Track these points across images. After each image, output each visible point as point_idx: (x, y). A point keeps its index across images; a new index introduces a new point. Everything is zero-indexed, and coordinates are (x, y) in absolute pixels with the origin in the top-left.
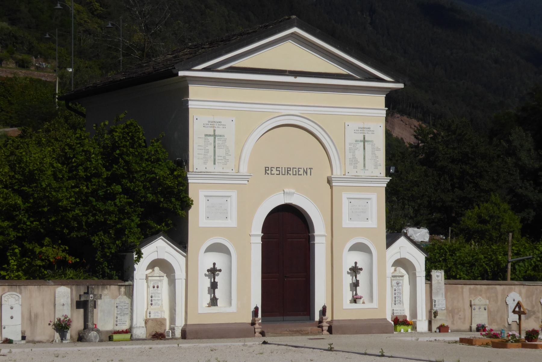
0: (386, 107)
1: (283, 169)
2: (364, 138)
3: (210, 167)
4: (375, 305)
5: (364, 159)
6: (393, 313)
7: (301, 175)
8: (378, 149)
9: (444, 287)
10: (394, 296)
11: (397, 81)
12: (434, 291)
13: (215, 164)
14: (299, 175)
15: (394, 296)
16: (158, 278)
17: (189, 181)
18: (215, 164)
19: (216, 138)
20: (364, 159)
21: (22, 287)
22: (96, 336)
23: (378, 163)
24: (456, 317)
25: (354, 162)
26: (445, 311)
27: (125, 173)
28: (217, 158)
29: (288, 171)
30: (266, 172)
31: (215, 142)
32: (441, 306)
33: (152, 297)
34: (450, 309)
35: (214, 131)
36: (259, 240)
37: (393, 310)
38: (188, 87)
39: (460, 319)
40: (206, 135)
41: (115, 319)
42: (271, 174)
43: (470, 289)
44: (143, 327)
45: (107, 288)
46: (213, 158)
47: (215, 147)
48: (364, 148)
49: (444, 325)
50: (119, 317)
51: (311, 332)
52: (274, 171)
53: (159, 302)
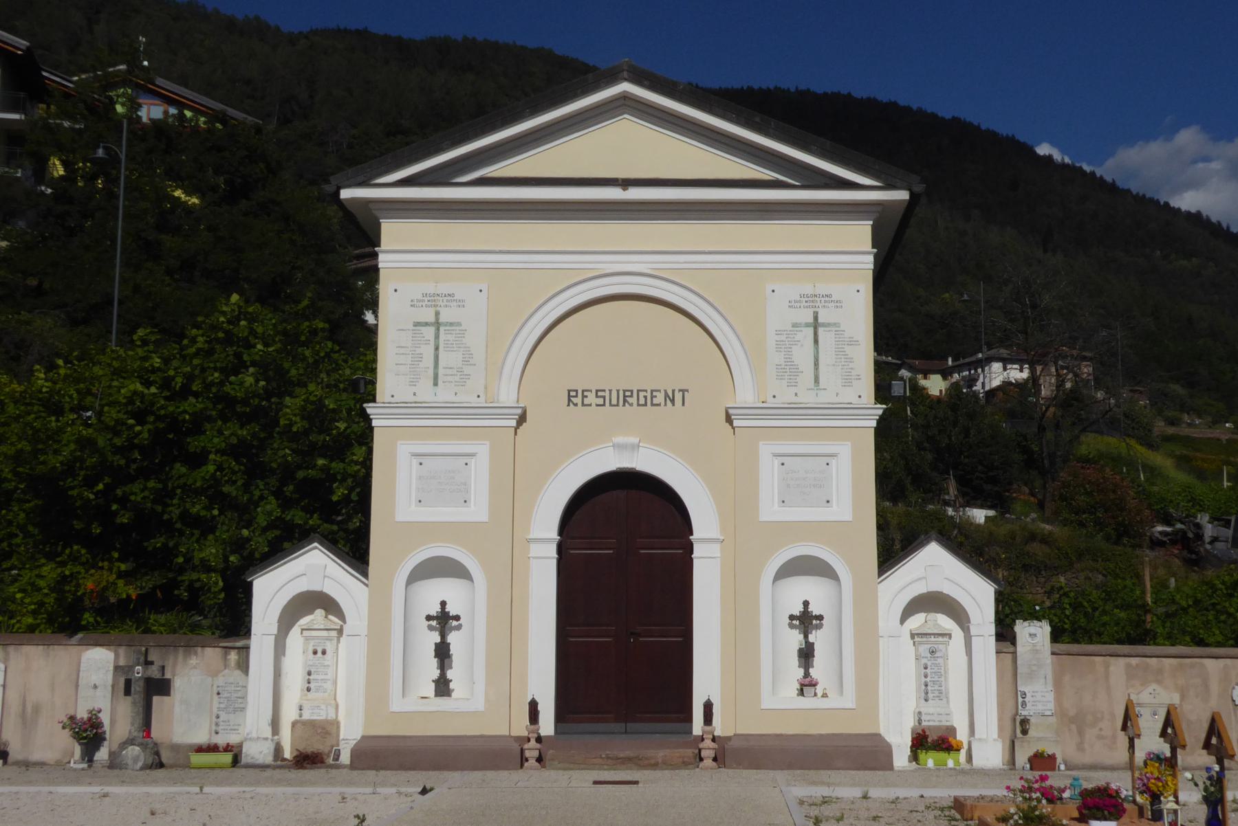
0: (873, 247)
1: (614, 394)
2: (816, 318)
3: (425, 392)
4: (848, 701)
5: (816, 364)
6: (920, 721)
7: (659, 405)
8: (853, 342)
9: (1049, 661)
10: (923, 680)
11: (889, 186)
12: (1021, 670)
13: (436, 384)
14: (653, 405)
15: (923, 680)
16: (325, 633)
17: (374, 423)
18: (436, 384)
19: (442, 329)
20: (816, 364)
21: (11, 649)
22: (138, 756)
23: (854, 373)
24: (1090, 734)
25: (789, 372)
26: (1053, 720)
27: (206, 409)
28: (441, 371)
29: (625, 396)
30: (569, 400)
31: (437, 337)
32: (1040, 707)
33: (309, 673)
34: (1072, 713)
35: (437, 314)
36: (552, 551)
37: (920, 713)
38: (379, 224)
39: (1100, 737)
40: (417, 324)
41: (214, 719)
42: (583, 404)
43: (1128, 666)
44: (266, 739)
45: (196, 654)
46: (431, 372)
47: (437, 349)
48: (816, 341)
49: (1042, 754)
50: (223, 716)
51: (664, 763)
52: (592, 398)
53: (328, 686)
